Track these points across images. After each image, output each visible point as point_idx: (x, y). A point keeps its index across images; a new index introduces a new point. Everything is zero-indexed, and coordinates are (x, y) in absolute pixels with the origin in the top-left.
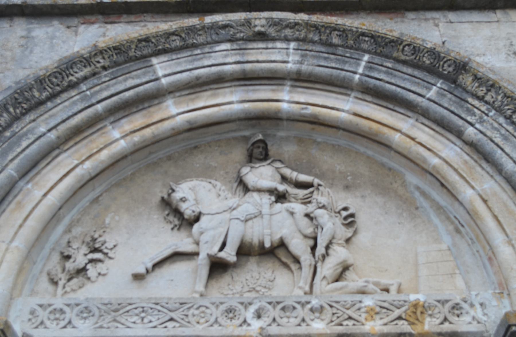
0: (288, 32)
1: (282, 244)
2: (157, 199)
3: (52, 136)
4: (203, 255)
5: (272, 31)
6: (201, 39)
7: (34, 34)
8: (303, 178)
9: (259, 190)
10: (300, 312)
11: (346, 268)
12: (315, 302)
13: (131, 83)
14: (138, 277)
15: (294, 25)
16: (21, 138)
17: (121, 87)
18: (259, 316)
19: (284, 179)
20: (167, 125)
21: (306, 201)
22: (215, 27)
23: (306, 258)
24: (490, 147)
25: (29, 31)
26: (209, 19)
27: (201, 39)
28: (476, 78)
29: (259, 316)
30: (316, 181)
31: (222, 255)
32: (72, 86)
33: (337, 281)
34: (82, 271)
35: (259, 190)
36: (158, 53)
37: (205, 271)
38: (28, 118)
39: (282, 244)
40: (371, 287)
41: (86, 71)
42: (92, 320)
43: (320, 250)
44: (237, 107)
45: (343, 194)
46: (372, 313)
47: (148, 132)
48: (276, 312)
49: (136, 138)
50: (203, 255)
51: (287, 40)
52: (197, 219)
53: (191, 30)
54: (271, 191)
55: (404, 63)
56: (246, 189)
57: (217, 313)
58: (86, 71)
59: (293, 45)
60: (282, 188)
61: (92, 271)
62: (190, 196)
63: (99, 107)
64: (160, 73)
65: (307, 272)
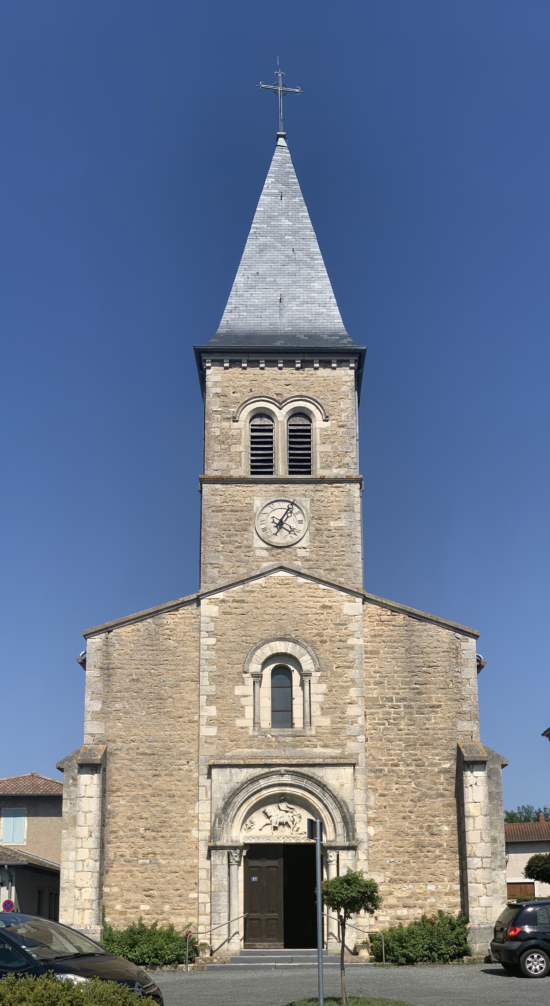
0: (289, 773)
1: (287, 823)
2: (262, 811)
3: (242, 802)
4: (272, 825)
5: (285, 773)
6: (270, 774)
7: (232, 772)
8: (292, 806)
9: (283, 810)
10: (290, 838)
11: (299, 828)
12: (293, 837)
13: (255, 787)
14: (260, 830)
15: (290, 772)
16: (235, 803)
17: (253, 788)
18: (283, 838)
19: (288, 807)
20: (264, 796)
21: (292, 812)
22: (273, 772)
23: (292, 826)
24: (328, 806)
25: (231, 770)
26: (272, 770)
27: (270, 774)
28: (328, 789)
29: (283, 838)
30: (294, 808)
31: (276, 826)
32: (244, 789)
33: (297, 831)
34: (250, 828)
35: (283, 810)
36: (260, 779)
37: (273, 829)
38: (236, 797)
39: (287, 823)
40: (303, 833)
41: (246, 785)
42: (254, 840)
43: (294, 825)
44: (278, 792)
45: (299, 810)
46: (303, 838)
47: (260, 798)
48: (286, 838)
49: (258, 800)
50: (272, 825)
51: (288, 774)
52: (271, 816)
53: (268, 773)
54: (285, 811)
55: (314, 782)
56: (280, 809)
57: (276, 838)
58: (246, 785)
59: (290, 776)
60: (287, 810)
61: (252, 828)
62: (269, 812)
63: (250, 794)
64: (262, 784)
65: (292, 829)
